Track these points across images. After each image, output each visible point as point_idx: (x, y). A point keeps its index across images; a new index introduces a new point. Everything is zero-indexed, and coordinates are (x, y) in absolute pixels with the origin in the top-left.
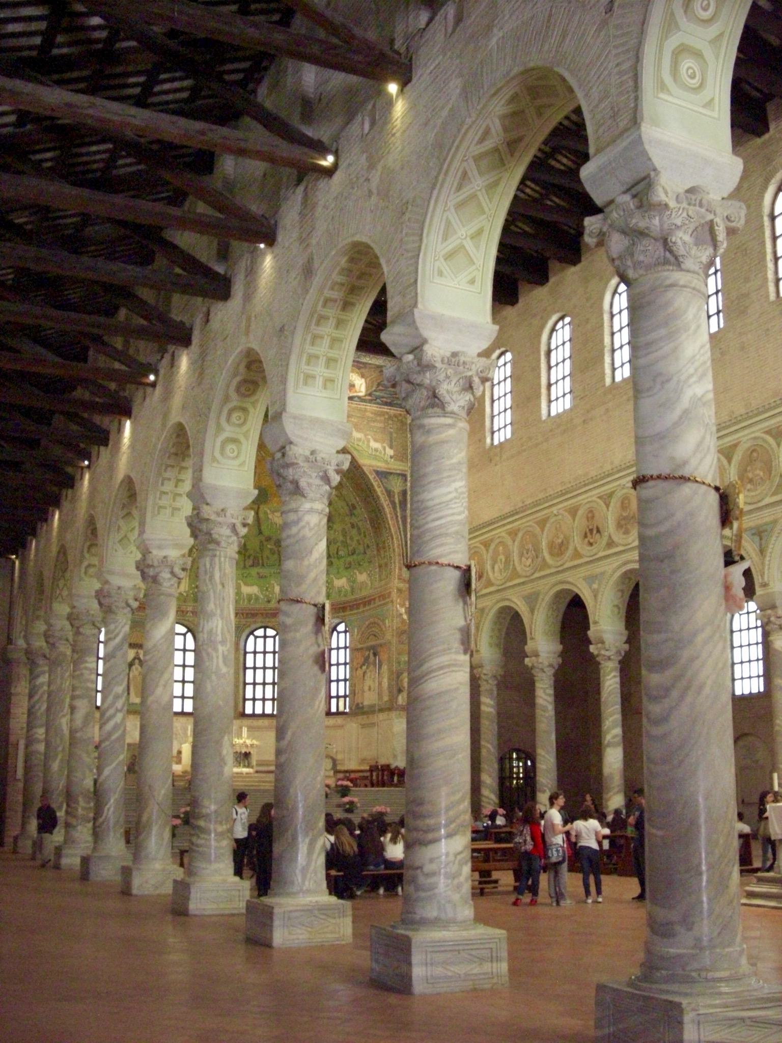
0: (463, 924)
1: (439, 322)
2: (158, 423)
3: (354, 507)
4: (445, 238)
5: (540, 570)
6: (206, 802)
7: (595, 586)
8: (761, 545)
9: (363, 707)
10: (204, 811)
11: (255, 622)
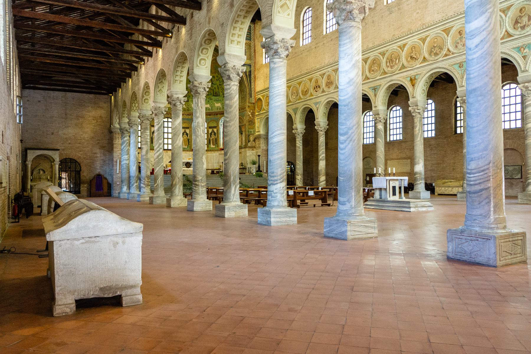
2: (174, 51)
5: (299, 100)
6: (198, 176)
7: (317, 106)
8: (375, 93)
10: (197, 179)
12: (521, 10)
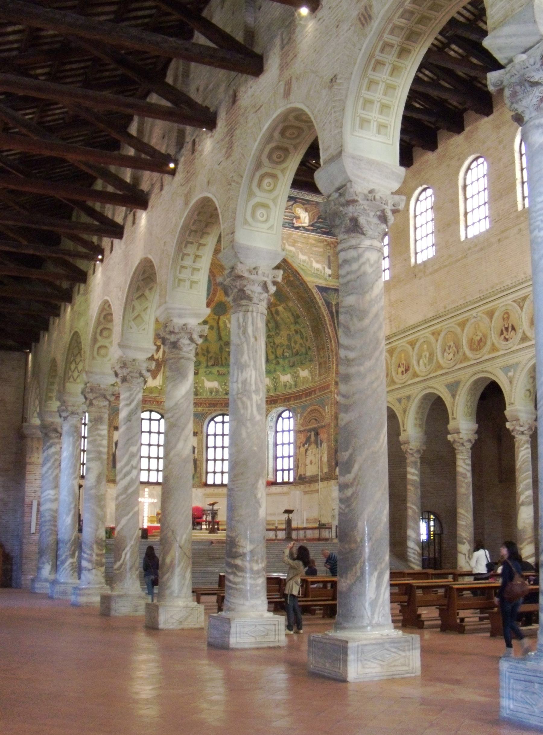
3: (298, 317)
6: (242, 542)
7: (511, 374)
9: (305, 478)
10: (241, 550)
11: (215, 410)
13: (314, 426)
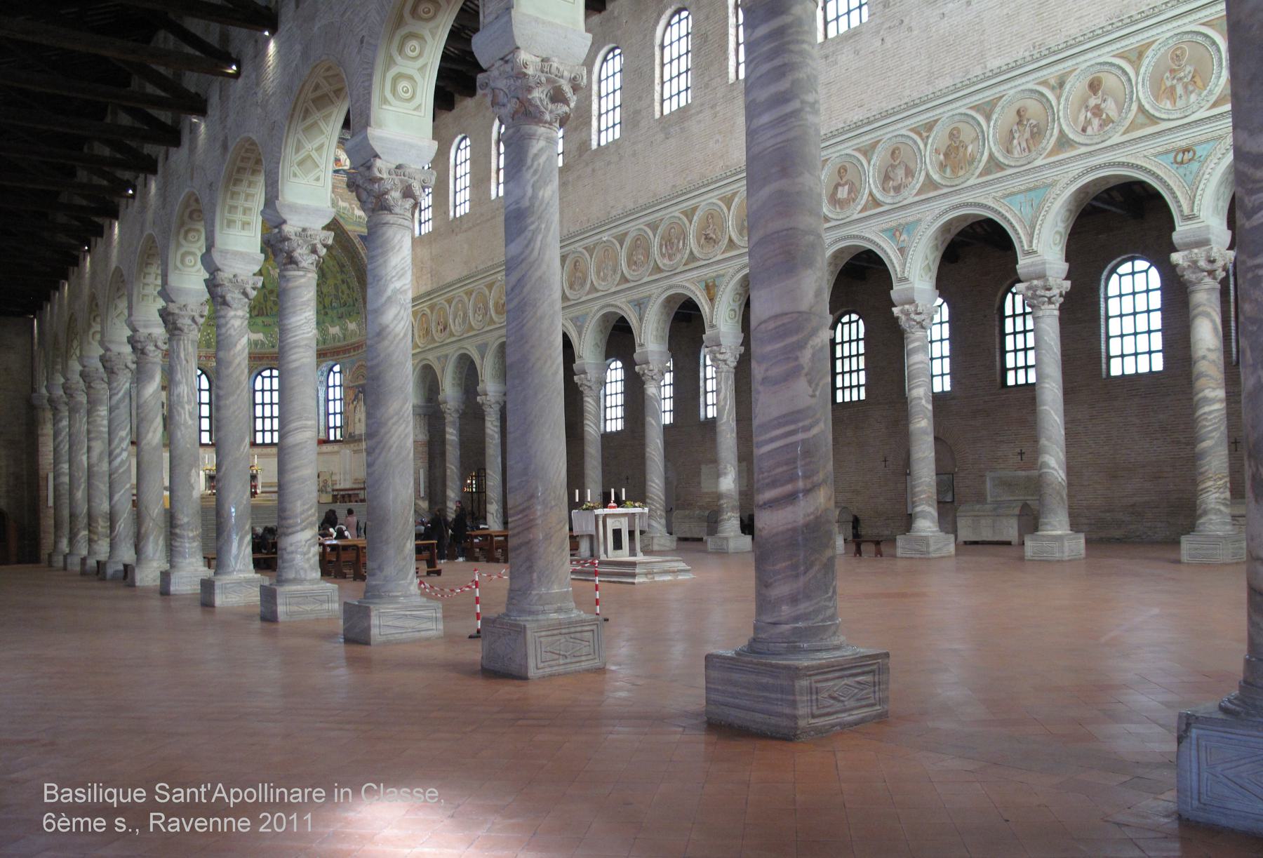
0: (312, 581)
1: (294, 208)
4: (298, 150)
5: (489, 325)
9: (354, 436)
10: (179, 522)
11: (261, 365)
12: (893, 153)
13: (361, 382)
